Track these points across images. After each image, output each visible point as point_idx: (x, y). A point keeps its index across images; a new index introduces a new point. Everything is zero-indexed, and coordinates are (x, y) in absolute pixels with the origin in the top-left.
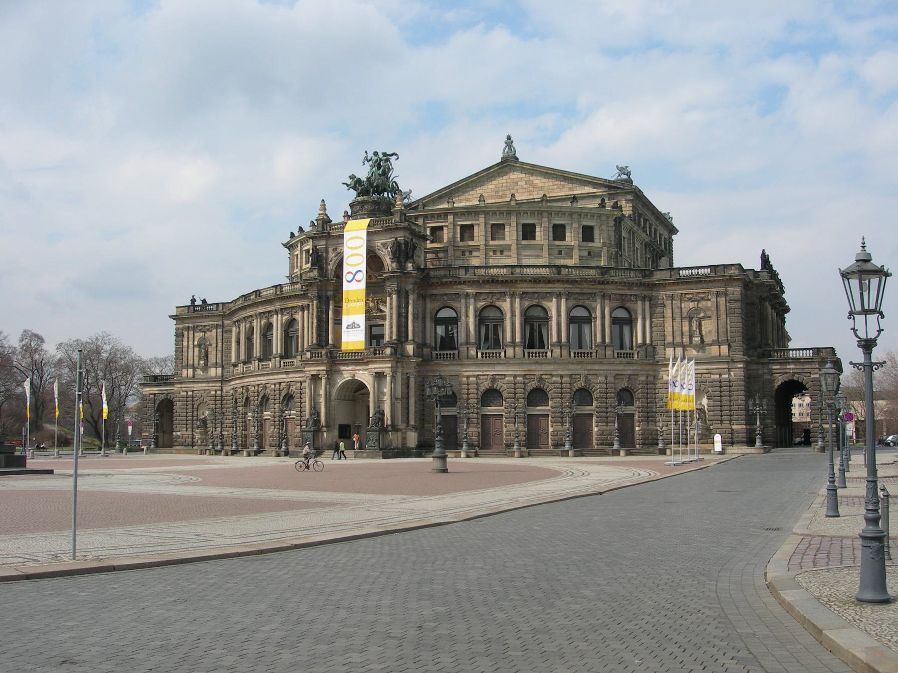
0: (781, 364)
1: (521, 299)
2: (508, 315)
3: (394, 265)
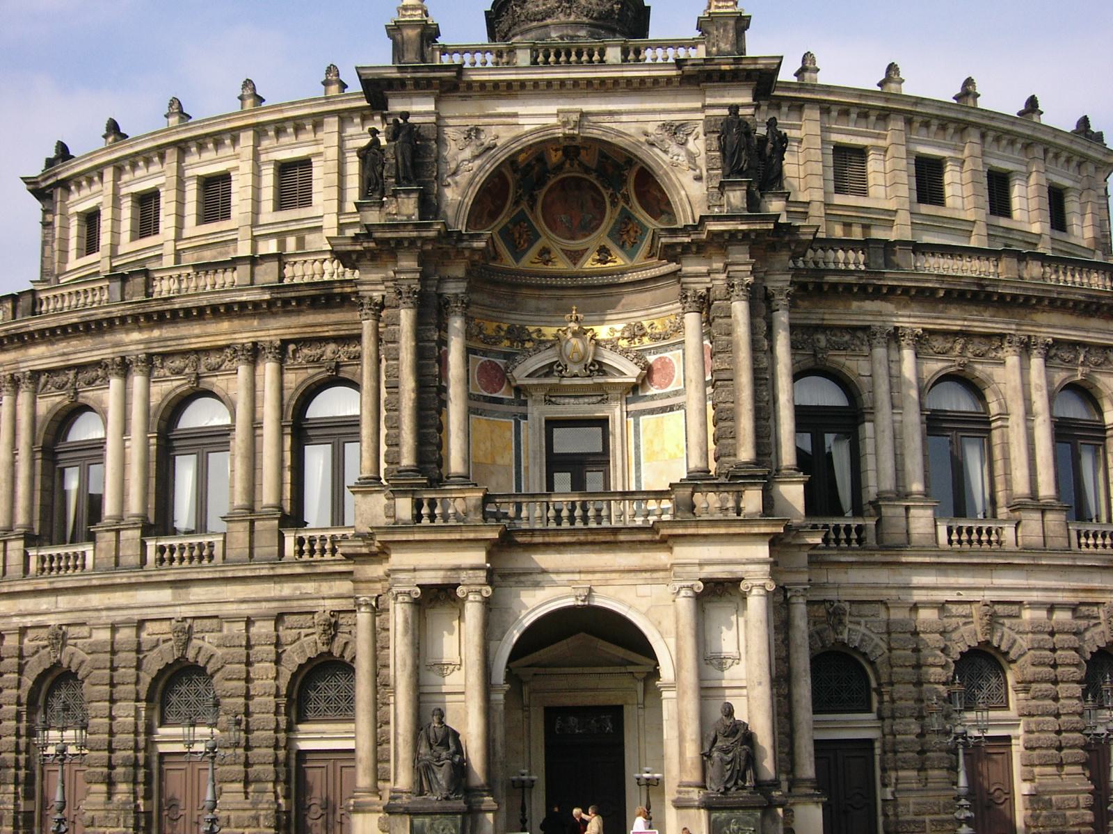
1: (1047, 358)
2: (1017, 409)
3: (736, 198)
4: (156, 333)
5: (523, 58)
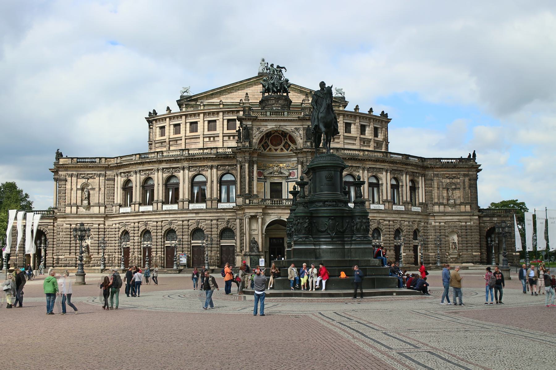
0: (489, 217)
3: (309, 144)
4: (190, 162)
5: (268, 113)
